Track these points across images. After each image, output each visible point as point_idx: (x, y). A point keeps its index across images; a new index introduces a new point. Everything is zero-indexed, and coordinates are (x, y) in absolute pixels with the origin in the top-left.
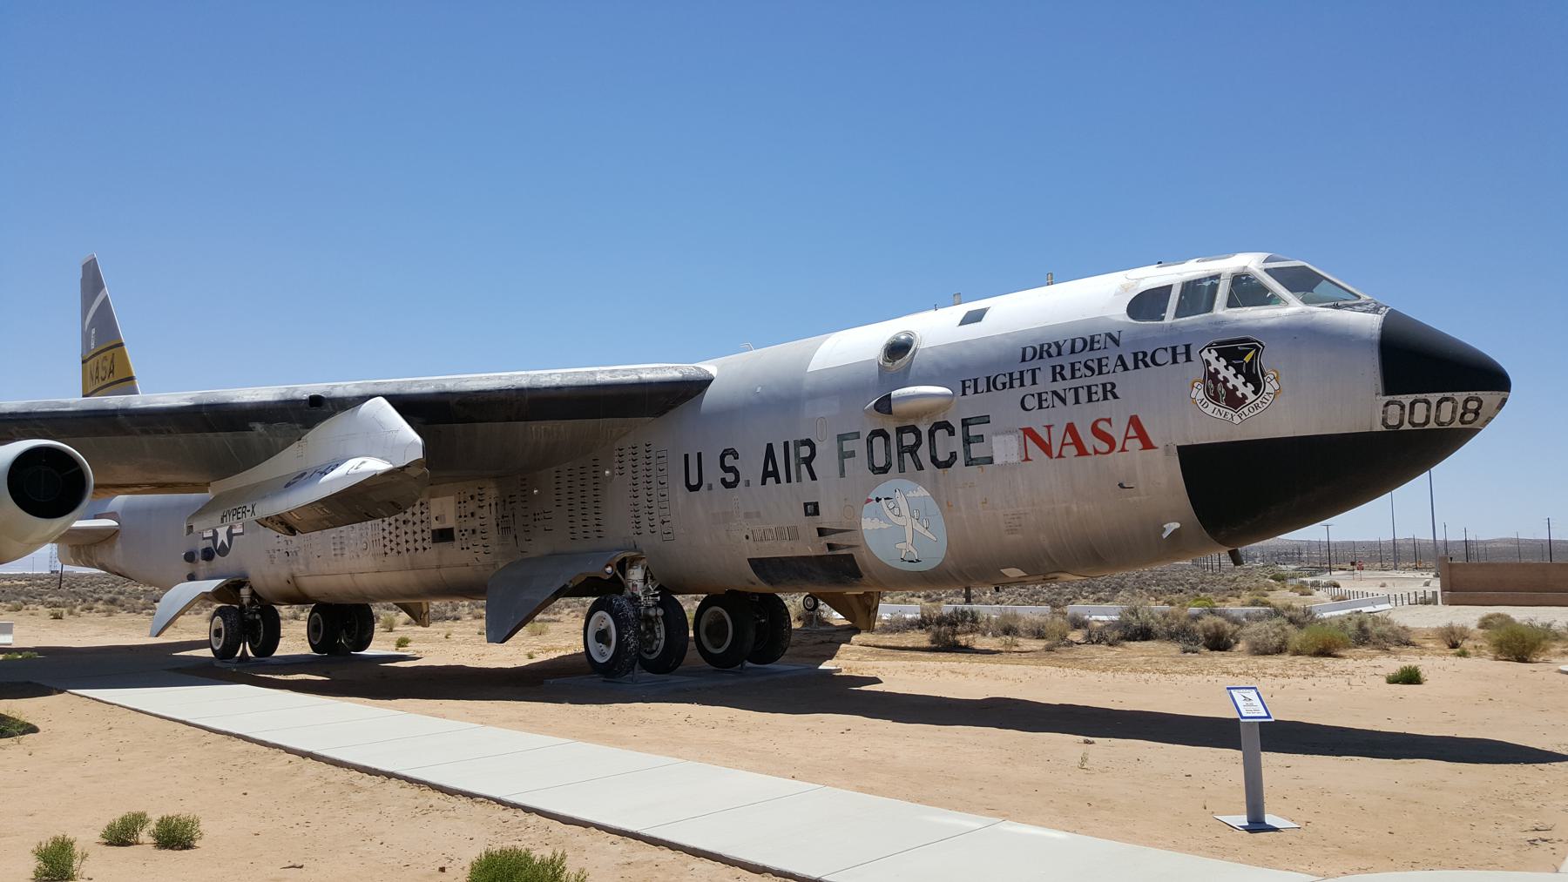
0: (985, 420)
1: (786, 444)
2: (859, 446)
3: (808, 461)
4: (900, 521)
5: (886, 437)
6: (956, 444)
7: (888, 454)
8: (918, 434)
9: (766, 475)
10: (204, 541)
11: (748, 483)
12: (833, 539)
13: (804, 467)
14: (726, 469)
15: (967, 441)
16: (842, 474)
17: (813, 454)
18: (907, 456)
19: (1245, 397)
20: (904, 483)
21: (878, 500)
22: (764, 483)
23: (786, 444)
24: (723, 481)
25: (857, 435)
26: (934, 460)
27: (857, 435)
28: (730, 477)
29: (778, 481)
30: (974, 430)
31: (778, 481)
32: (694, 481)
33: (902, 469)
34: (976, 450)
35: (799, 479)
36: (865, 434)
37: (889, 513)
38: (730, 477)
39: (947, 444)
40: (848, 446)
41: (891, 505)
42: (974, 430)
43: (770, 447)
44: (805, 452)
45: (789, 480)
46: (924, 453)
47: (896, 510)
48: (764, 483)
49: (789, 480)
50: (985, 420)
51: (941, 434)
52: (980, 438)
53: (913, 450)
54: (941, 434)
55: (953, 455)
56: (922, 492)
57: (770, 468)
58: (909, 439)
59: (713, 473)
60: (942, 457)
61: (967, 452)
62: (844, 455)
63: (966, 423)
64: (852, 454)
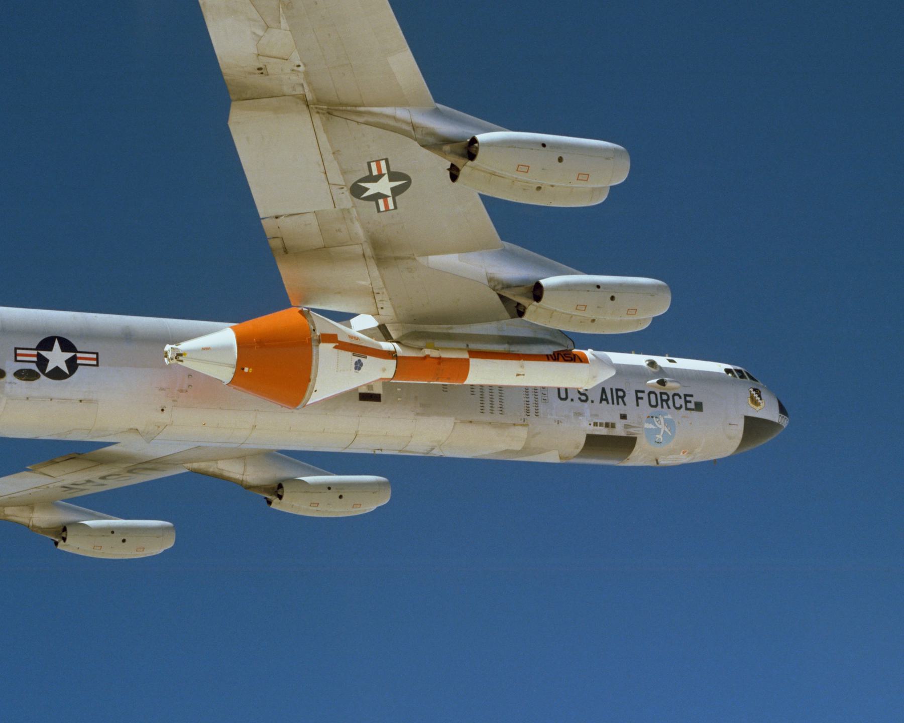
0: (692, 396)
2: (645, 396)
3: (623, 397)
4: (660, 426)
5: (656, 395)
6: (682, 402)
7: (657, 402)
9: (602, 400)
11: (592, 402)
13: (620, 400)
15: (686, 402)
16: (638, 405)
17: (624, 395)
19: (760, 403)
21: (652, 417)
22: (601, 402)
23: (611, 389)
24: (580, 399)
25: (643, 392)
27: (643, 392)
28: (583, 398)
30: (688, 399)
33: (662, 407)
35: (618, 403)
36: (647, 392)
37: (656, 423)
38: (583, 398)
39: (679, 402)
40: (640, 395)
41: (658, 420)
42: (688, 399)
43: (603, 390)
44: (621, 394)
45: (613, 403)
46: (670, 403)
47: (659, 422)
48: (601, 402)
49: (613, 403)
50: (692, 396)
51: (676, 398)
53: (667, 401)
54: (676, 398)
55: (681, 406)
57: (604, 397)
58: (665, 397)
60: (677, 405)
62: (638, 398)
64: (641, 398)
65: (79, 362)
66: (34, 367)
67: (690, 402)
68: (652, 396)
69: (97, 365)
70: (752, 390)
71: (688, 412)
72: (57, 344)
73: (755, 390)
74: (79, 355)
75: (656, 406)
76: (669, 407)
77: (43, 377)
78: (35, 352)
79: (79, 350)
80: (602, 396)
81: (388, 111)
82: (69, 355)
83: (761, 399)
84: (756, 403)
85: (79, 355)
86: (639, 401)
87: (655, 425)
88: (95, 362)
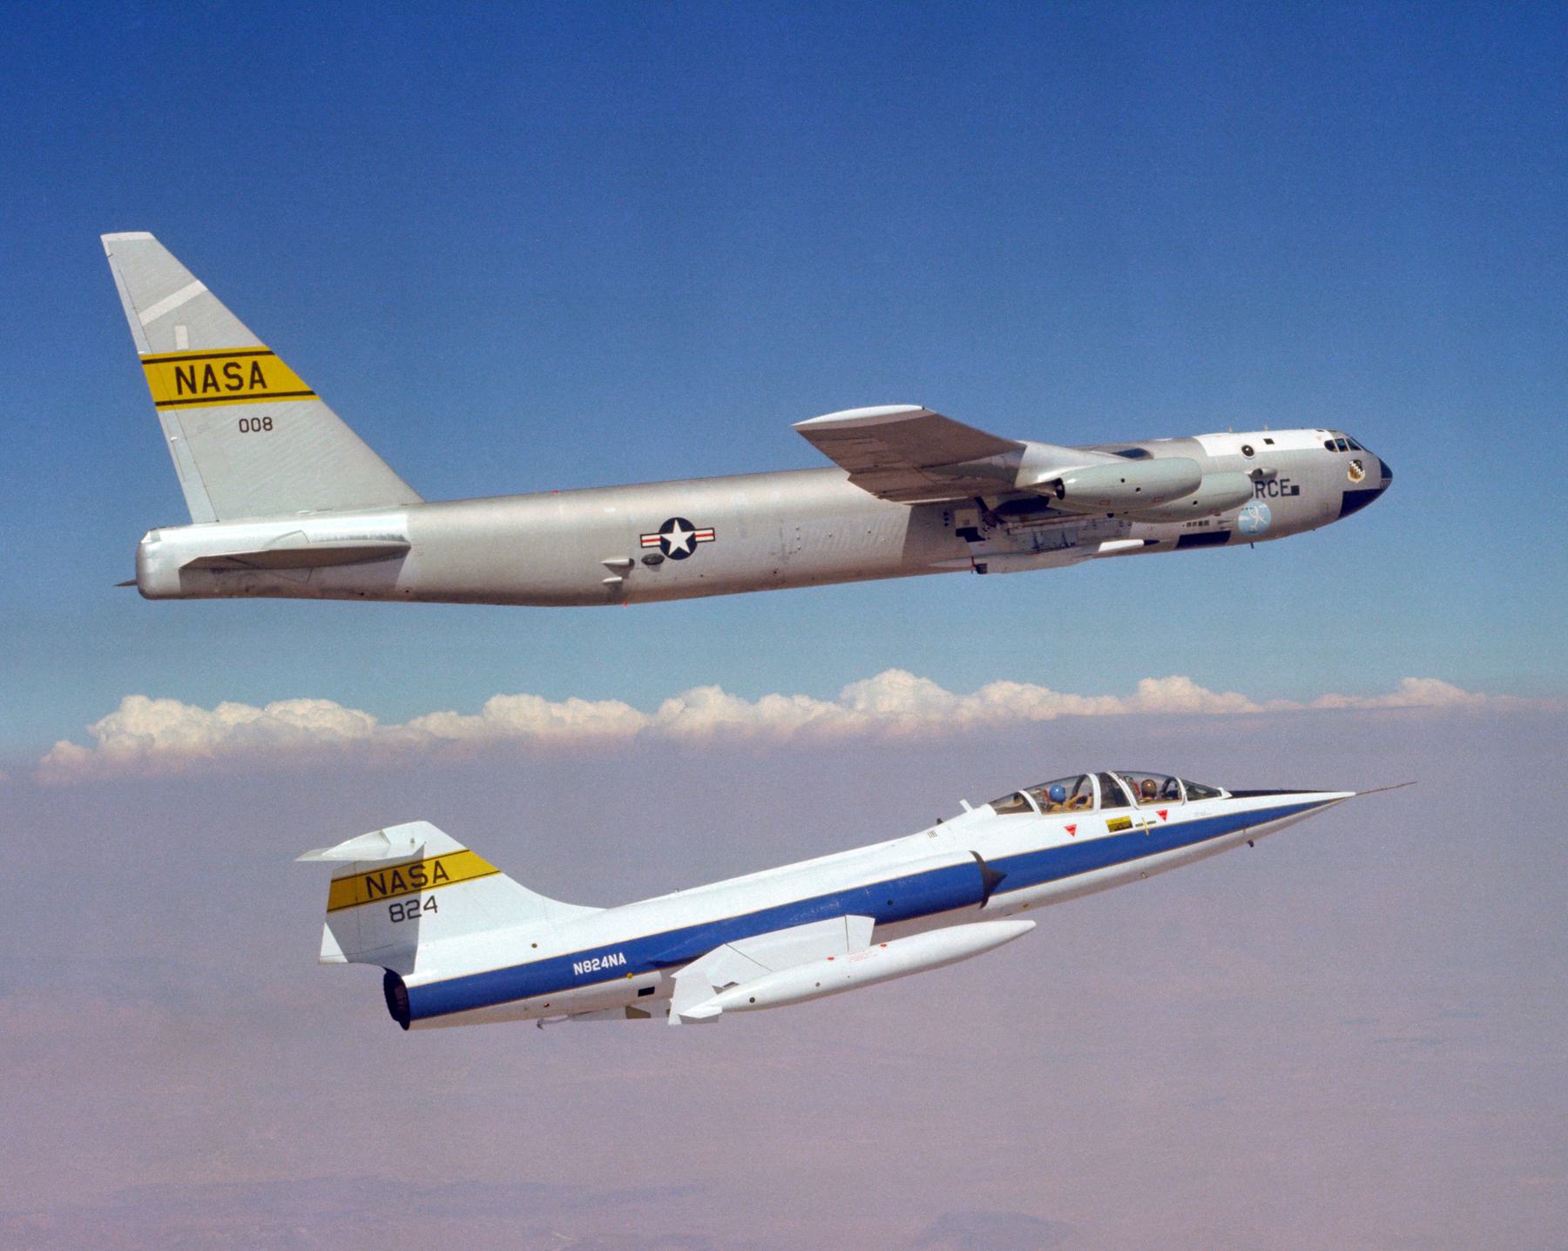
0: (1288, 480)
10: (643, 550)
12: (1225, 525)
15: (1282, 487)
18: (1260, 493)
20: (1257, 502)
30: (1284, 484)
33: (1257, 497)
42: (1284, 484)
46: (1266, 491)
50: (1288, 480)
53: (1262, 490)
55: (1277, 493)
56: (1264, 506)
61: (1282, 491)
65: (697, 539)
66: (659, 551)
67: (1286, 487)
69: (714, 540)
70: (1352, 462)
71: (1286, 498)
72: (677, 526)
73: (1355, 462)
74: (697, 533)
76: (1264, 496)
77: (666, 558)
78: (658, 537)
79: (696, 527)
81: (986, 460)
82: (688, 534)
83: (1362, 470)
84: (1355, 475)
85: (697, 533)
87: (1248, 515)
88: (711, 538)
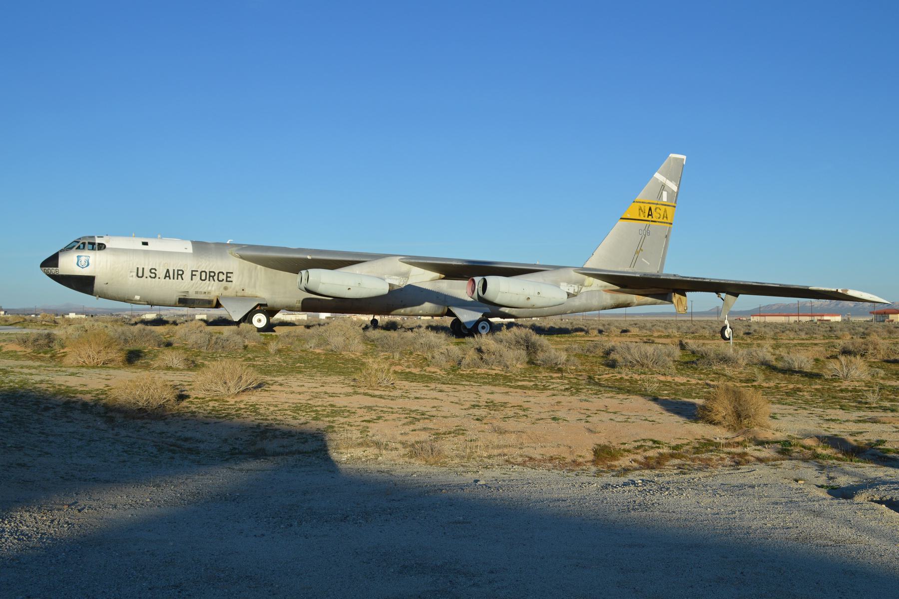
0: (232, 273)
1: (174, 270)
2: (198, 274)
3: (181, 275)
5: (206, 273)
8: (215, 273)
9: (166, 277)
14: (151, 273)
15: (227, 277)
16: (192, 280)
18: (211, 278)
22: (165, 278)
23: (174, 270)
25: (197, 271)
26: (218, 279)
27: (197, 271)
28: (153, 275)
29: (170, 279)
30: (229, 275)
31: (170, 279)
32: (140, 275)
34: (229, 279)
38: (153, 275)
39: (222, 277)
40: (194, 273)
42: (229, 275)
43: (168, 271)
44: (180, 272)
45: (174, 279)
46: (216, 278)
48: (165, 278)
49: (174, 279)
50: (232, 273)
51: (221, 274)
52: (230, 277)
53: (213, 277)
54: (221, 274)
55: (223, 280)
57: (168, 275)
58: (212, 274)
59: (147, 273)
60: (220, 279)
62: (192, 275)
63: (227, 273)
64: (195, 275)
68: (203, 274)
75: (204, 280)
80: (166, 274)
86: (193, 277)
